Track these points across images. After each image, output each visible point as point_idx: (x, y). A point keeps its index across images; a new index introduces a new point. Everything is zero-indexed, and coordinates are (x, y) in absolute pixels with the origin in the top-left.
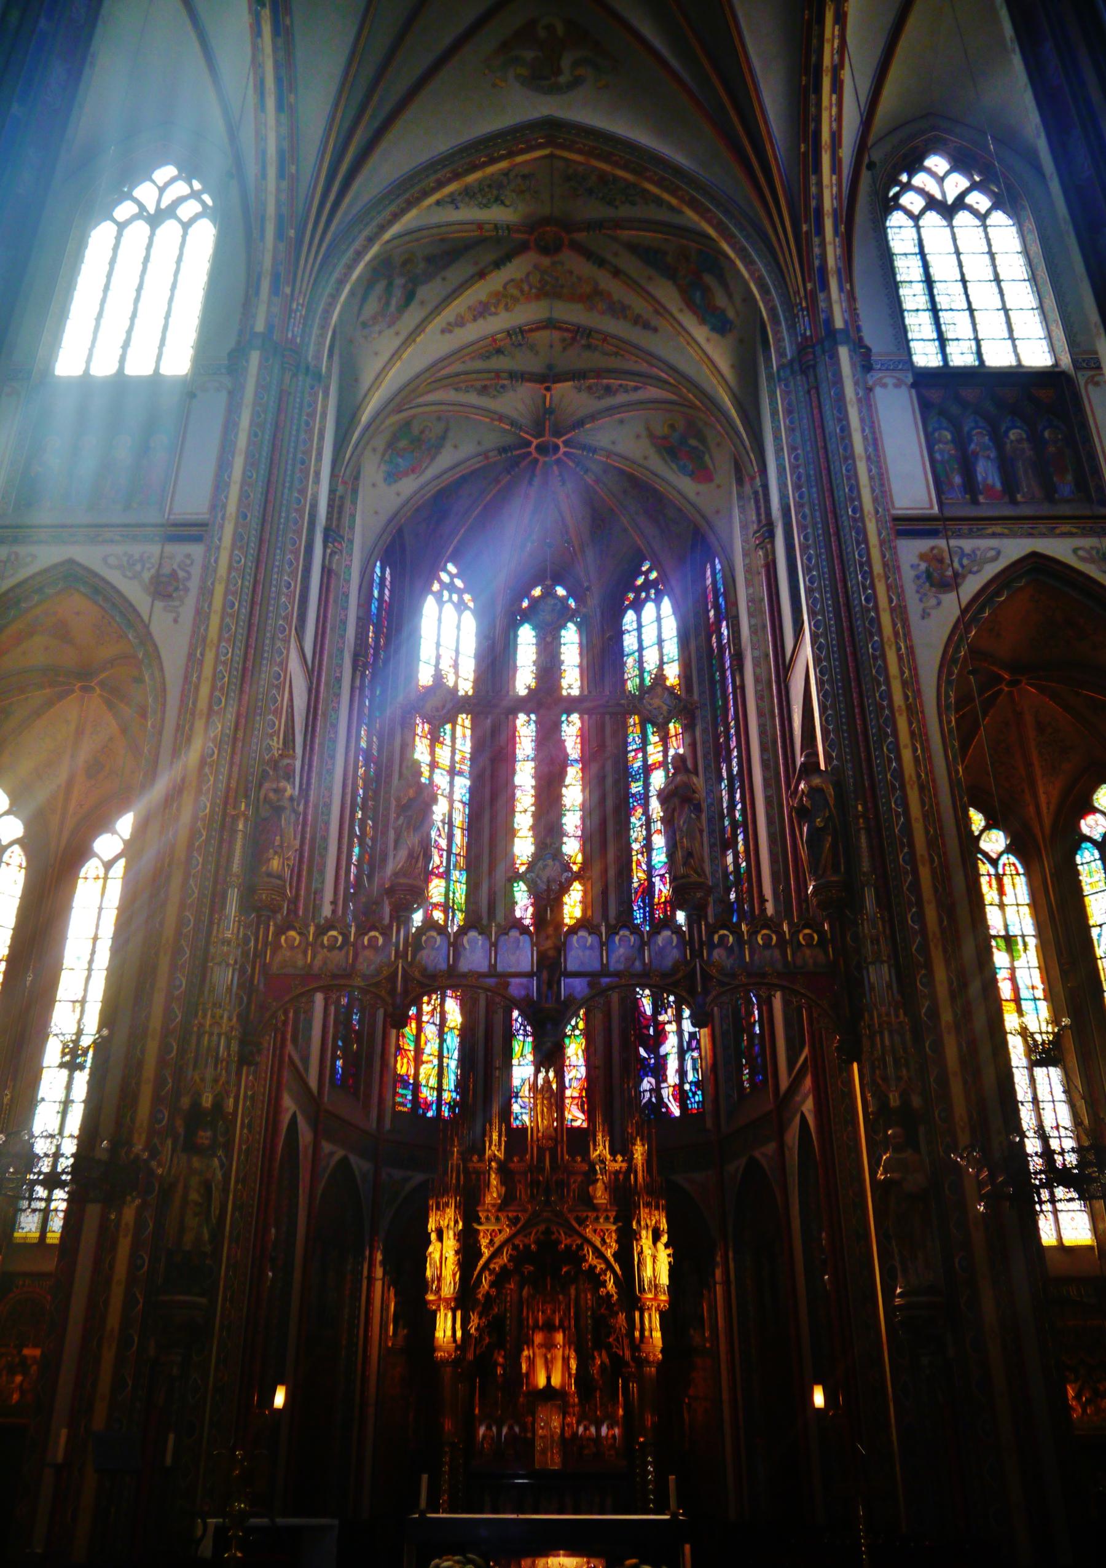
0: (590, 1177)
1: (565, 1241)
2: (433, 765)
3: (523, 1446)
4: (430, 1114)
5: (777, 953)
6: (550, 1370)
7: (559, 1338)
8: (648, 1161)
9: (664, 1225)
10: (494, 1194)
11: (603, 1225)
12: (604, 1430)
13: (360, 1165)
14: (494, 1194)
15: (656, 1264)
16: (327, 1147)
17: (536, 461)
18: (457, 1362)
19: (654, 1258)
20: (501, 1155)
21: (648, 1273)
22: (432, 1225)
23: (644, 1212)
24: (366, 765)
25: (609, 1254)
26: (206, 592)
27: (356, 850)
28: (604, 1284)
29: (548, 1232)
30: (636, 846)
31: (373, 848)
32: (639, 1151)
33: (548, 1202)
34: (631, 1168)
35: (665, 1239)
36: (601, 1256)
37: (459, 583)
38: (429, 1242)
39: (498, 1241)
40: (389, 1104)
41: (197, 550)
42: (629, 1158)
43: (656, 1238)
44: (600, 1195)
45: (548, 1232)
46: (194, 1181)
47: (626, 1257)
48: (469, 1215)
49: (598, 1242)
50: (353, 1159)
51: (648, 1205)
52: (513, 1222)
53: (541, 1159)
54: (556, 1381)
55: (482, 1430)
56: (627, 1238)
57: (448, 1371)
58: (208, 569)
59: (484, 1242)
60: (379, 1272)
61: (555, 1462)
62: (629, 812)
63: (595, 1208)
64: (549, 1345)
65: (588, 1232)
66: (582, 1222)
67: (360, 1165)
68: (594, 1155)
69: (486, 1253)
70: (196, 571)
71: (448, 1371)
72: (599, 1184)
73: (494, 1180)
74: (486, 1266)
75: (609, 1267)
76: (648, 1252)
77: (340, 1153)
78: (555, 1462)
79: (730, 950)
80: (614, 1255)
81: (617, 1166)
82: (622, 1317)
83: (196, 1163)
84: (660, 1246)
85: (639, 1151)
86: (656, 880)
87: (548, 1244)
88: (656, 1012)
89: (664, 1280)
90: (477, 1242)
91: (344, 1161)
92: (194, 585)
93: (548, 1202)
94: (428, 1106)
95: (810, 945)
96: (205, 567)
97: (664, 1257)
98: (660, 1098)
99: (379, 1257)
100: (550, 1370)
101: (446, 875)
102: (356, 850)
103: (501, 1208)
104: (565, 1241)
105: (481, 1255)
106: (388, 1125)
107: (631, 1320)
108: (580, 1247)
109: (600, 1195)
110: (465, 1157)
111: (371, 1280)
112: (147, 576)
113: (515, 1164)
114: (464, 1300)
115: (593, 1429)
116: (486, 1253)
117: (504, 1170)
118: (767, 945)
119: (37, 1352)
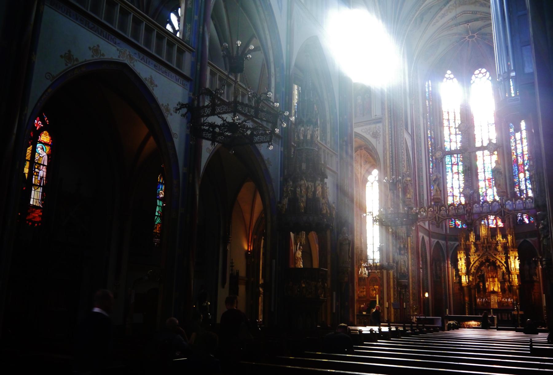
0: (497, 244)
1: (492, 259)
2: (450, 134)
3: (488, 303)
4: (459, 227)
5: (522, 205)
6: (495, 286)
7: (496, 279)
8: (512, 240)
9: (517, 254)
10: (473, 249)
11: (501, 255)
12: (509, 300)
13: (442, 242)
14: (473, 249)
15: (515, 264)
16: (433, 240)
17: (469, 41)
18: (467, 287)
19: (515, 263)
20: (474, 241)
21: (513, 266)
22: (459, 257)
23: (511, 252)
24: (431, 141)
25: (503, 262)
26: (384, 137)
27: (431, 164)
28: (502, 269)
29: (487, 258)
30: (512, 148)
31: (436, 162)
32: (510, 238)
33: (487, 251)
34: (508, 242)
35: (517, 258)
36: (501, 262)
37: (452, 76)
38: (458, 261)
39: (475, 260)
40: (448, 226)
41: (380, 125)
42: (507, 239)
43: (515, 258)
44: (500, 248)
45: (487, 258)
46: (402, 260)
47: (507, 262)
48: (467, 255)
49: (500, 259)
50: (440, 241)
51: (512, 251)
52: (478, 255)
53: (484, 241)
54: (496, 289)
55: (478, 300)
56: (507, 258)
57: (465, 288)
58: (384, 131)
59: (472, 260)
60: (450, 266)
61: (496, 306)
62: (510, 138)
63: (499, 252)
64: (494, 281)
65: (497, 257)
66: (495, 255)
67: (442, 242)
68: (497, 239)
69: (472, 263)
70: (381, 130)
71: (465, 288)
72: (500, 247)
73: (473, 246)
74: (472, 266)
75: (503, 265)
76: (512, 262)
77: (436, 240)
78: (496, 306)
79: (510, 205)
80: (505, 262)
81: (504, 242)
82: (507, 276)
83: (402, 257)
84: (516, 260)
85: (510, 238)
86: (519, 158)
87: (487, 260)
88: (521, 195)
89: (518, 267)
90: (470, 260)
91: (438, 242)
92: (381, 133)
93: (487, 251)
94: (459, 225)
95: (530, 203)
96: (383, 130)
97: (517, 263)
98: (523, 219)
99: (450, 262)
100: (495, 286)
101: (457, 164)
102: (431, 164)
103: (475, 253)
104: (492, 259)
105: (471, 263)
106: (448, 232)
107: (509, 277)
108: (496, 261)
109: (500, 248)
110: (465, 241)
111: (448, 267)
112: (371, 133)
113: (478, 242)
114: (468, 273)
115: (506, 300)
116: (472, 263)
117: (475, 244)
118: (519, 204)
119: (377, 287)
